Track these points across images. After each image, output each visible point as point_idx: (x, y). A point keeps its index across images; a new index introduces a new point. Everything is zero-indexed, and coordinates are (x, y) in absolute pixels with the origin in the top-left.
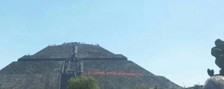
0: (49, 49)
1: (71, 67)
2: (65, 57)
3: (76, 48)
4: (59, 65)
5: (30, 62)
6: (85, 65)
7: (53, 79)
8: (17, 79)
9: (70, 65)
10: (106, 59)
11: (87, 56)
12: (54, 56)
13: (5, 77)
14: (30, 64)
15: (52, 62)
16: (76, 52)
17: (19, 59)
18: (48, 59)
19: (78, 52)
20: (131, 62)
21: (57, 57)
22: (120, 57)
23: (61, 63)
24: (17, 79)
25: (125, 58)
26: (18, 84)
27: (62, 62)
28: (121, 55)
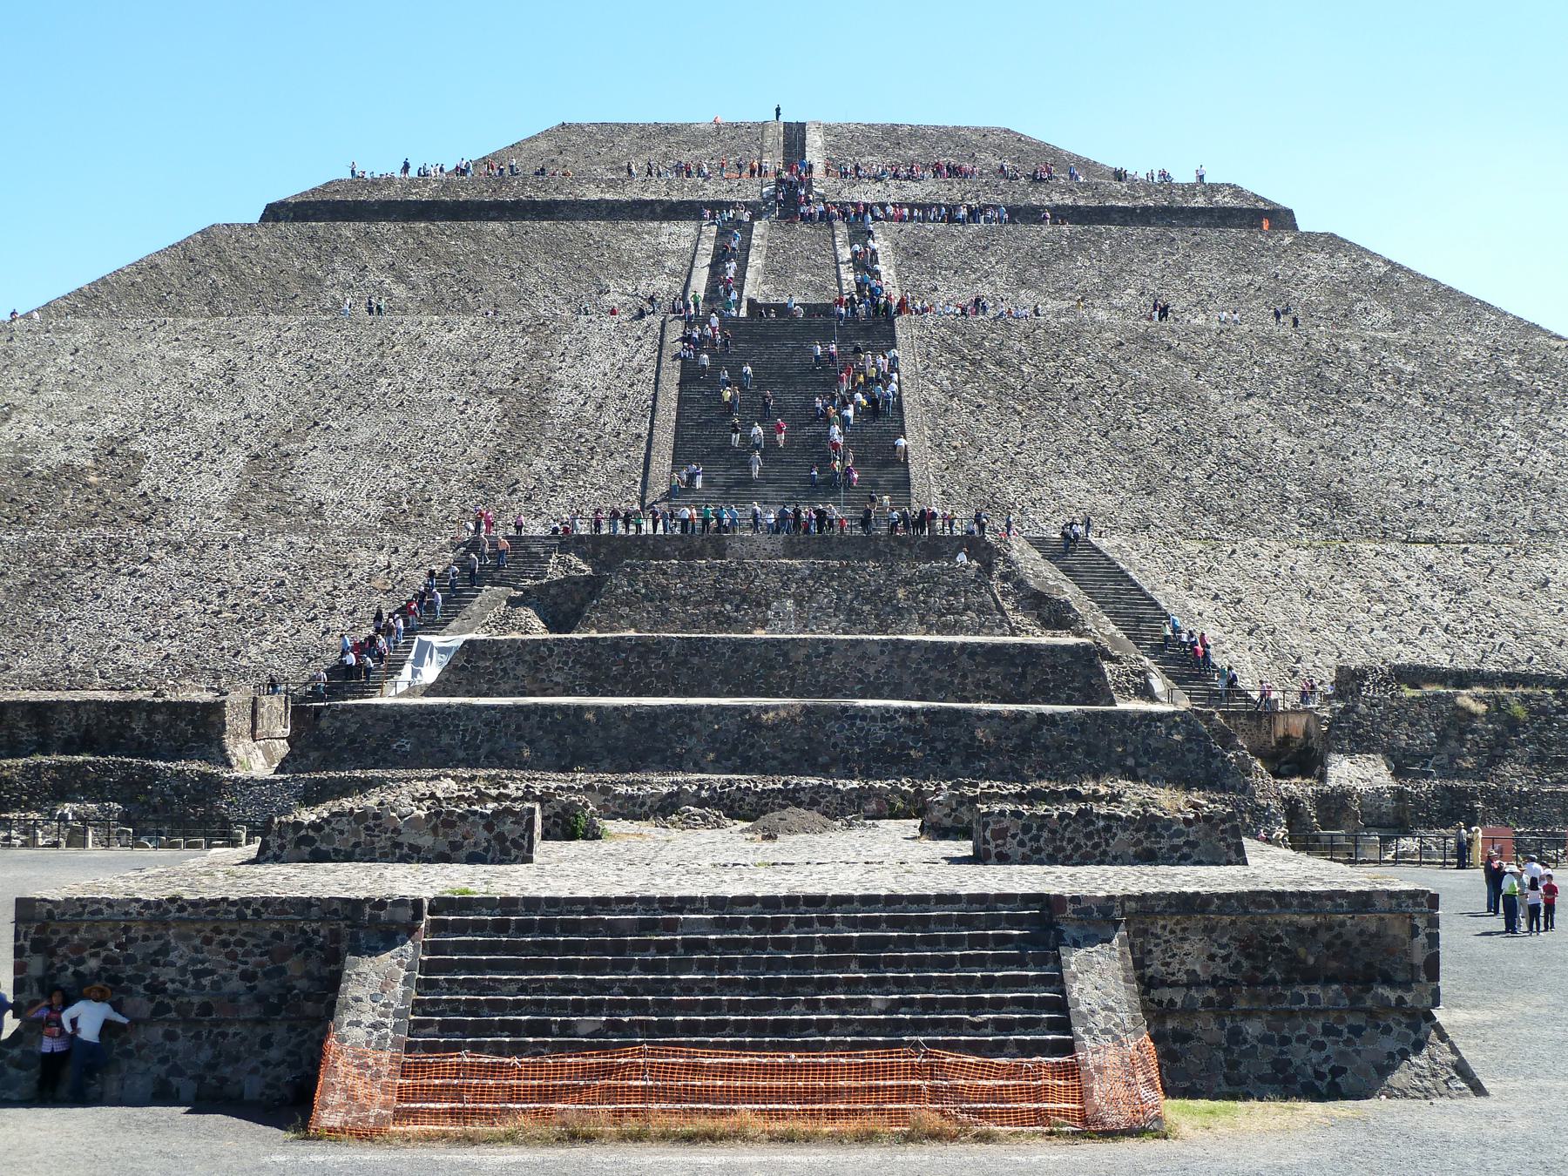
1: (775, 272)
4: (657, 258)
5: (385, 226)
8: (203, 363)
9: (772, 252)
10: (1103, 215)
12: (612, 184)
13: (79, 339)
17: (274, 213)
18: (548, 210)
20: (1333, 243)
22: (1225, 200)
24: (203, 363)
25: (1282, 218)
27: (687, 228)
28: (1237, 192)
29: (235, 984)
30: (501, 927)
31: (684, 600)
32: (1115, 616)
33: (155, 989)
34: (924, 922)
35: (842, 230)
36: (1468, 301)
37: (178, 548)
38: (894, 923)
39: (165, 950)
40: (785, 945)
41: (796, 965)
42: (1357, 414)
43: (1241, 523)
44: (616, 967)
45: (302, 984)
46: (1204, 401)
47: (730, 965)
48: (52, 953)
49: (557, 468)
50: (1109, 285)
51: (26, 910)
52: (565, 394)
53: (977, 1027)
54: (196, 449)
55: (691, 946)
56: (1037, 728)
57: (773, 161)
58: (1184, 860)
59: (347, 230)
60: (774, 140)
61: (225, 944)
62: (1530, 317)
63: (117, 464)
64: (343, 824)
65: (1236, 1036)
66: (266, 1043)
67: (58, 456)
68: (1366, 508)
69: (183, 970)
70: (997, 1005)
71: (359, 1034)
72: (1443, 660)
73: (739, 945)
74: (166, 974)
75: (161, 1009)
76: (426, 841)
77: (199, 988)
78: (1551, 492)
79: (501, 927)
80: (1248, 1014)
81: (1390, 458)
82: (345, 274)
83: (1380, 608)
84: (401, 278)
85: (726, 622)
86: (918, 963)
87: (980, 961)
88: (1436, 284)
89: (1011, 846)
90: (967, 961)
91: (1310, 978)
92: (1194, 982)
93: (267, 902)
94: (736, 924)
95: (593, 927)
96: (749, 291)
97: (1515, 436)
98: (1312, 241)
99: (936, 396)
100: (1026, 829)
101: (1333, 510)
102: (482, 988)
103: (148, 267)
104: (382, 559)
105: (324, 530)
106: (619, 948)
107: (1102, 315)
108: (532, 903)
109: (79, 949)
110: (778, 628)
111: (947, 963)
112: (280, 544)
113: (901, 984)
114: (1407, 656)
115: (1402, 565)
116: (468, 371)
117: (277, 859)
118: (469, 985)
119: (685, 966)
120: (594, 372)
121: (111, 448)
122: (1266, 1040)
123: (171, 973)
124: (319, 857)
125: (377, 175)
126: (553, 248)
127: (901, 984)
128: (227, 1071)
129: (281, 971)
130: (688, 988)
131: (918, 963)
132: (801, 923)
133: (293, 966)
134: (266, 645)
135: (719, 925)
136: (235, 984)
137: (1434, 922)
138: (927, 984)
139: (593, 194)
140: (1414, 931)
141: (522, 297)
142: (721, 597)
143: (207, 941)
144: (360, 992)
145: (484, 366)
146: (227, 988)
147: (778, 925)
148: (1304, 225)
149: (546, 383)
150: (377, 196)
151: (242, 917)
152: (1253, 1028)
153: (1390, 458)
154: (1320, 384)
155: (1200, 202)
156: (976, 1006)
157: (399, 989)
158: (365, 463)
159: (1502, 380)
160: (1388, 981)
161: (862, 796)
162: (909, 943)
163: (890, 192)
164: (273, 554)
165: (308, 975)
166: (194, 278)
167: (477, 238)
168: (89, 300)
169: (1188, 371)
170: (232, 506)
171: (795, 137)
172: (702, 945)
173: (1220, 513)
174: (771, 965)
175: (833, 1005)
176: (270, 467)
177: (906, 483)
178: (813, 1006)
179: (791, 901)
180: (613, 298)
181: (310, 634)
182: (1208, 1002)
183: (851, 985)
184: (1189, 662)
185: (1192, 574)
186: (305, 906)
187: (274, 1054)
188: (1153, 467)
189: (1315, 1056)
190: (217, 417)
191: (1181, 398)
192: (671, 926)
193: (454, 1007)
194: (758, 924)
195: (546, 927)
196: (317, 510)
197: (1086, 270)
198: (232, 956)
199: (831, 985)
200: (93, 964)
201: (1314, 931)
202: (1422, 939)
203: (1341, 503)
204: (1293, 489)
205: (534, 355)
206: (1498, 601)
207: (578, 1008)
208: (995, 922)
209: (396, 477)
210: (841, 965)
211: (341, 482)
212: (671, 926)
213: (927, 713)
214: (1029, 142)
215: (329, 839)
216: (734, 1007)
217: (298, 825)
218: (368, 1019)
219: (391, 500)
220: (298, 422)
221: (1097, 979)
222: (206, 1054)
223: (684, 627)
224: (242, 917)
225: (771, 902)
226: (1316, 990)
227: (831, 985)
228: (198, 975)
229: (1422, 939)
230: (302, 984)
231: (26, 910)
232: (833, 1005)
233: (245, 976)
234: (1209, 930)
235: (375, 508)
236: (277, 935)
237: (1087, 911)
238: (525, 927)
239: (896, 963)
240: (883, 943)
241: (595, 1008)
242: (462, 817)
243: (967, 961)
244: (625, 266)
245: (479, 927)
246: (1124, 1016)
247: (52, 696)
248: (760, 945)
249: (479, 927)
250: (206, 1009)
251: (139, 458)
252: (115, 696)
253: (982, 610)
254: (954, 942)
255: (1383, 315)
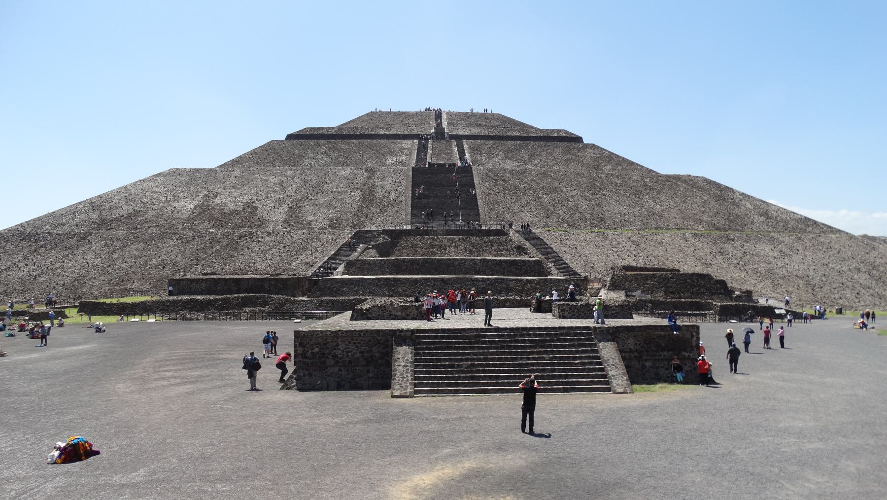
0: (371, 116)
2: (415, 131)
3: (444, 116)
4: (402, 150)
5: (322, 141)
6: (472, 149)
7: (389, 180)
11: (475, 131)
12: (387, 129)
14: (318, 145)
15: (383, 141)
16: (445, 124)
17: (290, 137)
19: (449, 123)
20: (593, 147)
21: (393, 132)
23: (407, 144)
24: (272, 180)
25: (578, 139)
26: (275, 191)
27: (409, 142)
28: (566, 132)
29: (358, 355)
30: (436, 337)
31: (422, 248)
32: (541, 252)
33: (335, 356)
34: (556, 335)
35: (454, 143)
36: (633, 163)
37: (270, 234)
38: (547, 335)
39: (338, 345)
40: (518, 341)
41: (522, 347)
42: (605, 195)
43: (573, 226)
44: (471, 348)
45: (377, 355)
46: (562, 191)
47: (503, 348)
48: (304, 346)
49: (378, 211)
50: (531, 159)
51: (297, 334)
52: (379, 190)
53: (576, 364)
54: (272, 205)
55: (490, 342)
56: (526, 284)
57: (433, 123)
58: (615, 317)
59: (312, 142)
60: (433, 116)
61: (355, 343)
62: (650, 168)
63: (249, 210)
64: (375, 309)
65: (644, 367)
66: (368, 372)
67: (231, 206)
68: (609, 222)
69: (343, 351)
70: (580, 358)
71: (400, 368)
72: (634, 264)
73: (505, 342)
74: (338, 352)
75: (337, 363)
76: (399, 314)
77: (348, 356)
78: (661, 216)
79: (436, 337)
80: (646, 360)
81: (615, 207)
82: (311, 154)
83: (615, 250)
84: (328, 156)
85: (434, 254)
86: (556, 346)
87: (573, 346)
88: (623, 158)
89: (566, 314)
90: (570, 346)
91: (663, 350)
92: (631, 351)
93: (367, 331)
94: (503, 336)
95: (462, 337)
96: (429, 160)
97: (650, 201)
98: (588, 145)
99: (486, 191)
100: (570, 309)
101: (598, 222)
102: (433, 355)
103: (254, 153)
104: (330, 237)
105: (310, 229)
106: (471, 343)
107: (530, 167)
108: (443, 330)
109: (313, 345)
110: (454, 254)
111: (565, 346)
112: (300, 232)
113: (552, 352)
114: (624, 263)
115: (622, 237)
116: (350, 182)
117: (356, 320)
118: (429, 354)
119: (490, 348)
120: (388, 184)
121: (248, 205)
122: (652, 367)
123: (340, 352)
124: (369, 319)
125: (475, 111)
126: (371, 147)
127: (552, 352)
128: (358, 380)
129: (371, 351)
130: (492, 354)
131: (556, 346)
132: (521, 335)
133: (374, 349)
134: (298, 262)
135: (498, 336)
136: (358, 355)
137: (698, 333)
138: (559, 352)
139: (382, 132)
140: (692, 336)
141: (364, 162)
142: (432, 247)
143: (350, 342)
144: (399, 356)
145: (356, 181)
146: (356, 356)
147: (515, 336)
148: (585, 142)
149: (374, 186)
150: (321, 132)
151: (360, 335)
152: (648, 364)
153: (615, 207)
154: (594, 188)
155: (556, 135)
156: (575, 358)
157: (410, 356)
158: (323, 209)
159: (645, 185)
160: (685, 350)
161: (506, 301)
162: (553, 341)
163: (467, 132)
164: (299, 235)
165: (379, 352)
166: (268, 155)
167: (349, 144)
168: (236, 162)
169: (556, 184)
170: (284, 221)
171: (438, 115)
172: (494, 342)
173: (568, 222)
174: (515, 347)
175: (534, 359)
176: (294, 212)
177: (478, 215)
178: (529, 359)
179: (518, 329)
180: (389, 162)
181: (310, 259)
182: (635, 357)
183: (538, 353)
184: (562, 266)
185: (561, 240)
186: (378, 332)
187: (371, 375)
188: (548, 210)
189: (666, 372)
190: (278, 196)
191: (555, 190)
192: (484, 337)
193: (426, 360)
194: (509, 336)
195: (449, 337)
196: (309, 223)
197: (524, 154)
198: (357, 347)
199: (532, 353)
200: (317, 349)
201: (664, 336)
202: (695, 338)
203: (602, 220)
204: (588, 216)
205: (370, 178)
206: (650, 249)
207: (462, 360)
208: (576, 334)
209: (332, 214)
210: (535, 347)
211: (316, 214)
212: (484, 337)
213: (495, 279)
214: (506, 117)
215: (371, 313)
216: (506, 359)
217: (362, 309)
218: (402, 364)
219: (331, 220)
220: (302, 198)
221: (608, 351)
222: (351, 376)
223: (422, 255)
224: (360, 335)
225: (512, 329)
226: (665, 353)
227: (532, 353)
228: (347, 352)
229: (695, 338)
230: (377, 355)
231: (297, 334)
232: (534, 359)
233: (361, 352)
234: (635, 336)
235: (326, 222)
236: (370, 341)
237: (603, 331)
238: (443, 337)
239: (550, 346)
240: (546, 341)
241: (467, 360)
242: (409, 306)
243: (570, 346)
244: (392, 153)
245: (429, 337)
246: (617, 361)
247: (240, 277)
248: (511, 342)
249: (429, 337)
250: (350, 362)
251: (256, 208)
252: (258, 277)
253: (507, 250)
254: (566, 340)
255: (609, 167)
